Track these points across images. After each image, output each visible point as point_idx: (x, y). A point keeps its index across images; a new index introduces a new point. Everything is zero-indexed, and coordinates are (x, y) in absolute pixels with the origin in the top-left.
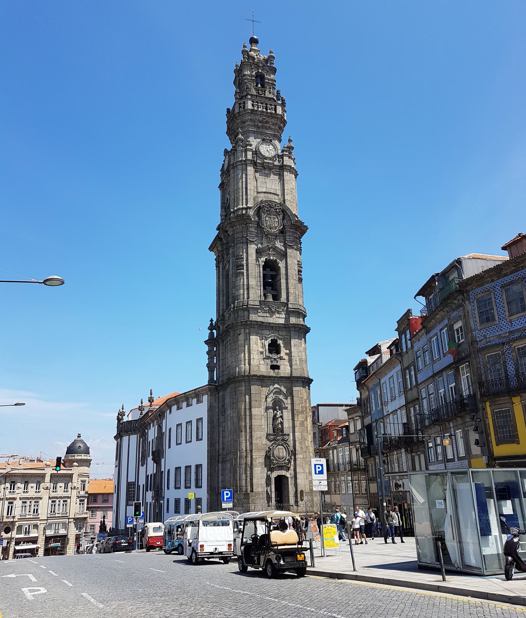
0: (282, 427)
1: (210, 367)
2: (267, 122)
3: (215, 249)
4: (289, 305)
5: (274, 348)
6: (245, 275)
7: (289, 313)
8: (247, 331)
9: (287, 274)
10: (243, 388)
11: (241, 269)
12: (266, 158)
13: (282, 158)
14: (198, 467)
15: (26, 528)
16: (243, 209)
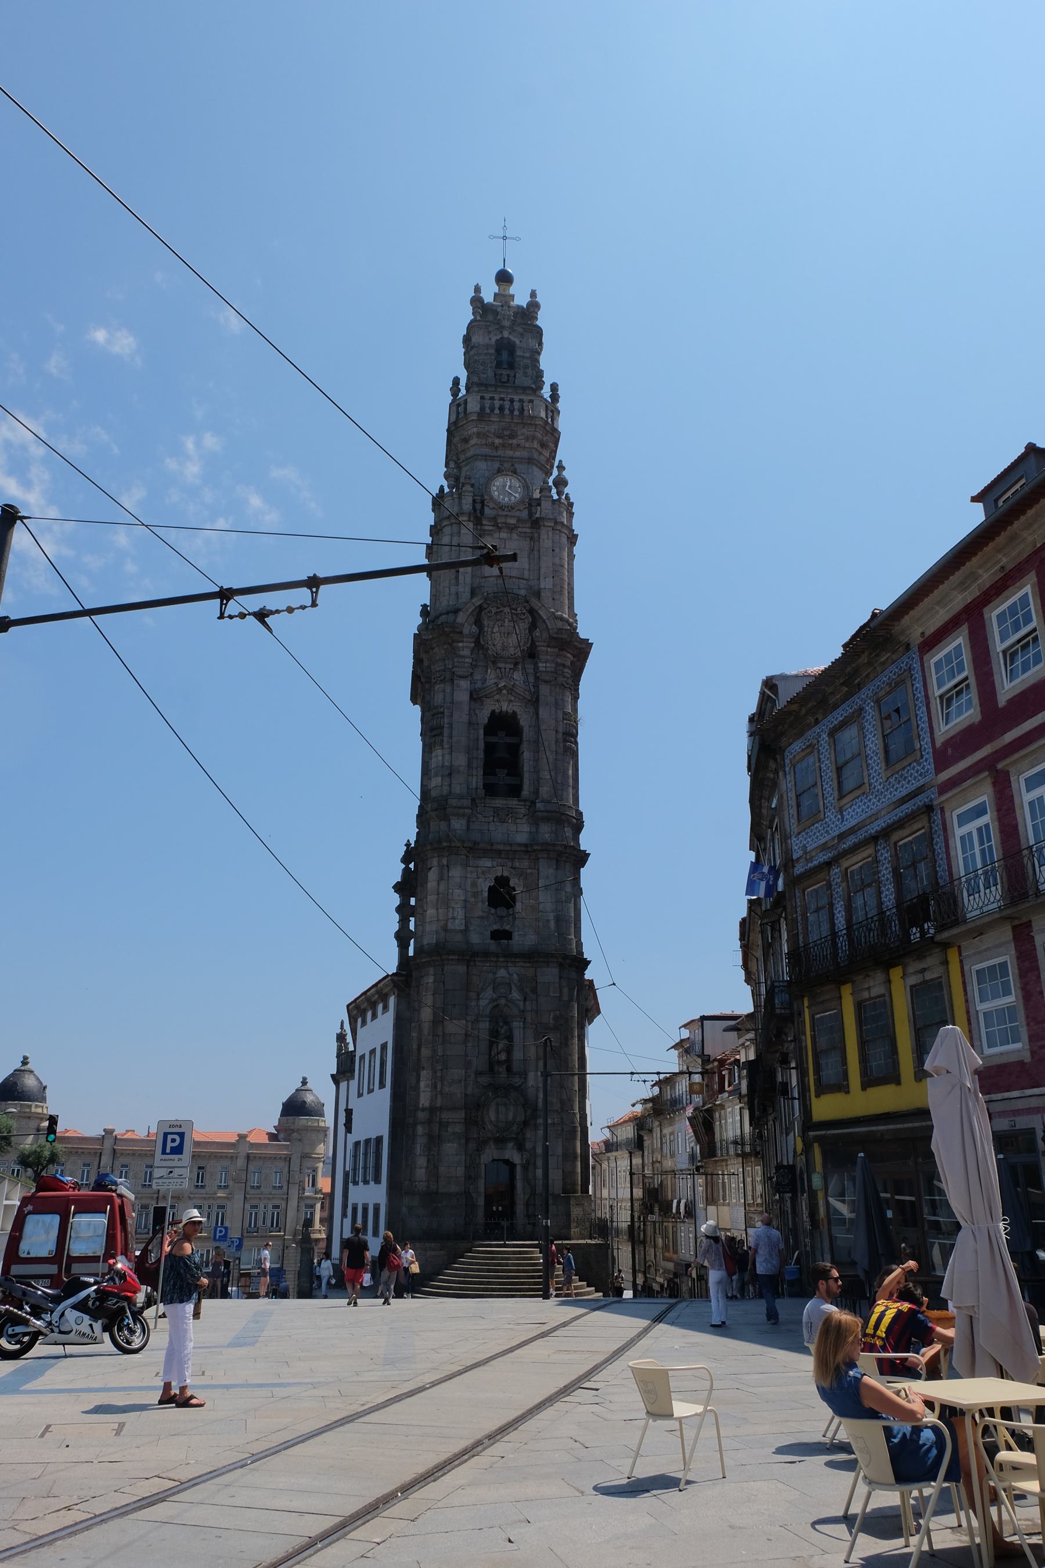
0: (509, 1061)
1: (402, 937)
2: (512, 436)
3: (419, 701)
4: (538, 805)
5: (501, 896)
6: (446, 746)
7: (535, 818)
8: (445, 861)
9: (536, 742)
10: (431, 979)
11: (438, 735)
12: (502, 508)
13: (539, 505)
14: (379, 1140)
15: (202, 1255)
16: (448, 613)
